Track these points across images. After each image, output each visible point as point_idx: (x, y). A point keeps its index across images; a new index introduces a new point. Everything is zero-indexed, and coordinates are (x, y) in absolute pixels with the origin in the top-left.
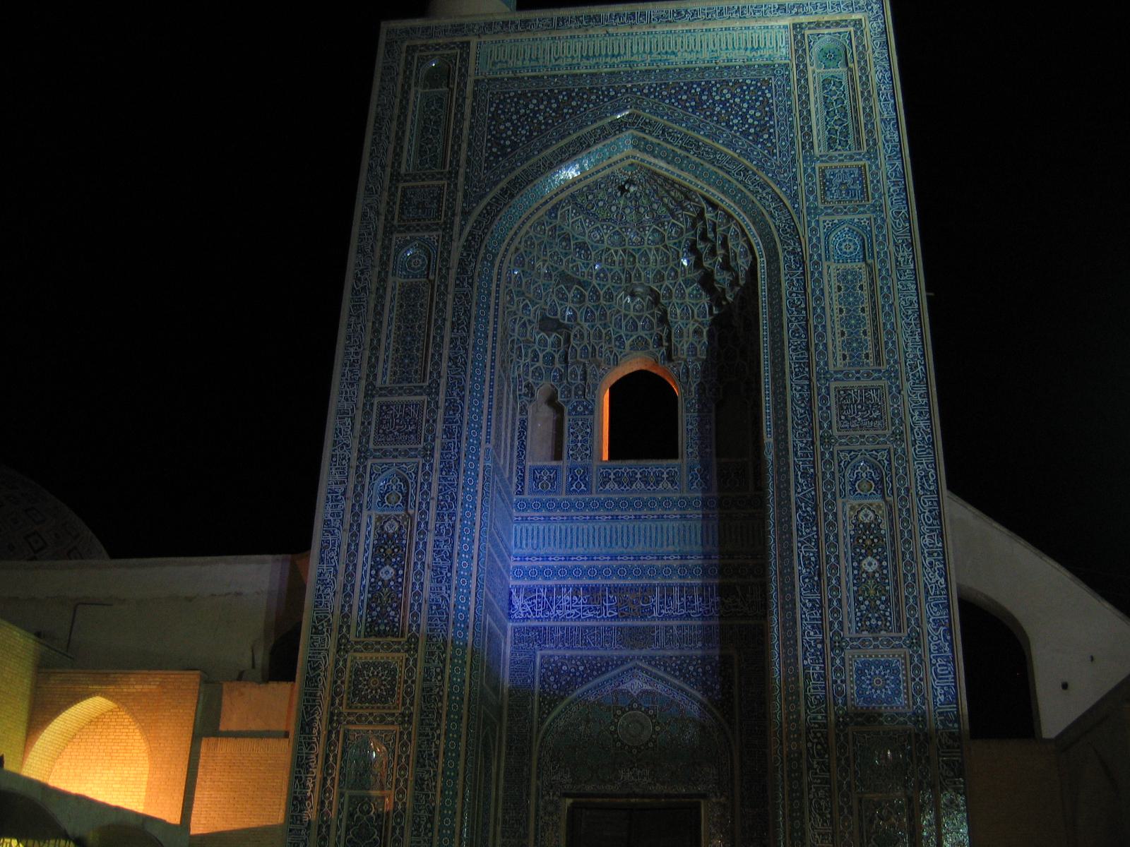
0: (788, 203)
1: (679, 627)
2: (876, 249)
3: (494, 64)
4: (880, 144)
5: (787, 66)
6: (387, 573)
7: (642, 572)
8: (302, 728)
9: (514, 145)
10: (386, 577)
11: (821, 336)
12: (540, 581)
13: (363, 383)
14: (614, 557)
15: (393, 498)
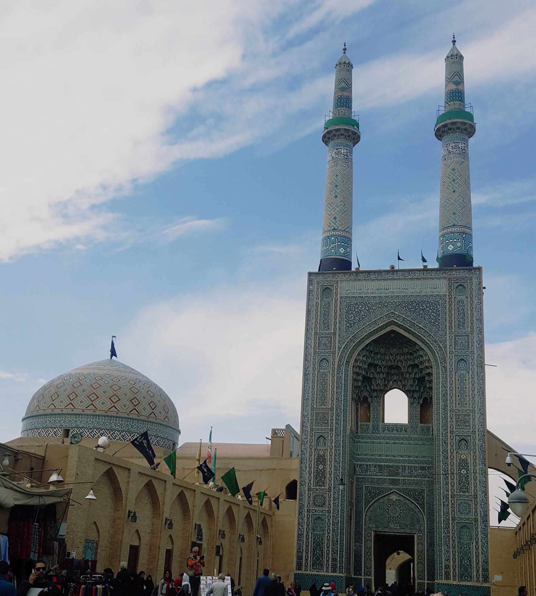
0: (443, 349)
1: (408, 480)
2: (471, 368)
3: (347, 290)
4: (475, 328)
5: (445, 295)
6: (321, 467)
7: (396, 461)
8: (299, 514)
9: (354, 323)
10: (321, 468)
11: (451, 397)
12: (364, 463)
13: (310, 406)
14: (387, 456)
15: (321, 444)
